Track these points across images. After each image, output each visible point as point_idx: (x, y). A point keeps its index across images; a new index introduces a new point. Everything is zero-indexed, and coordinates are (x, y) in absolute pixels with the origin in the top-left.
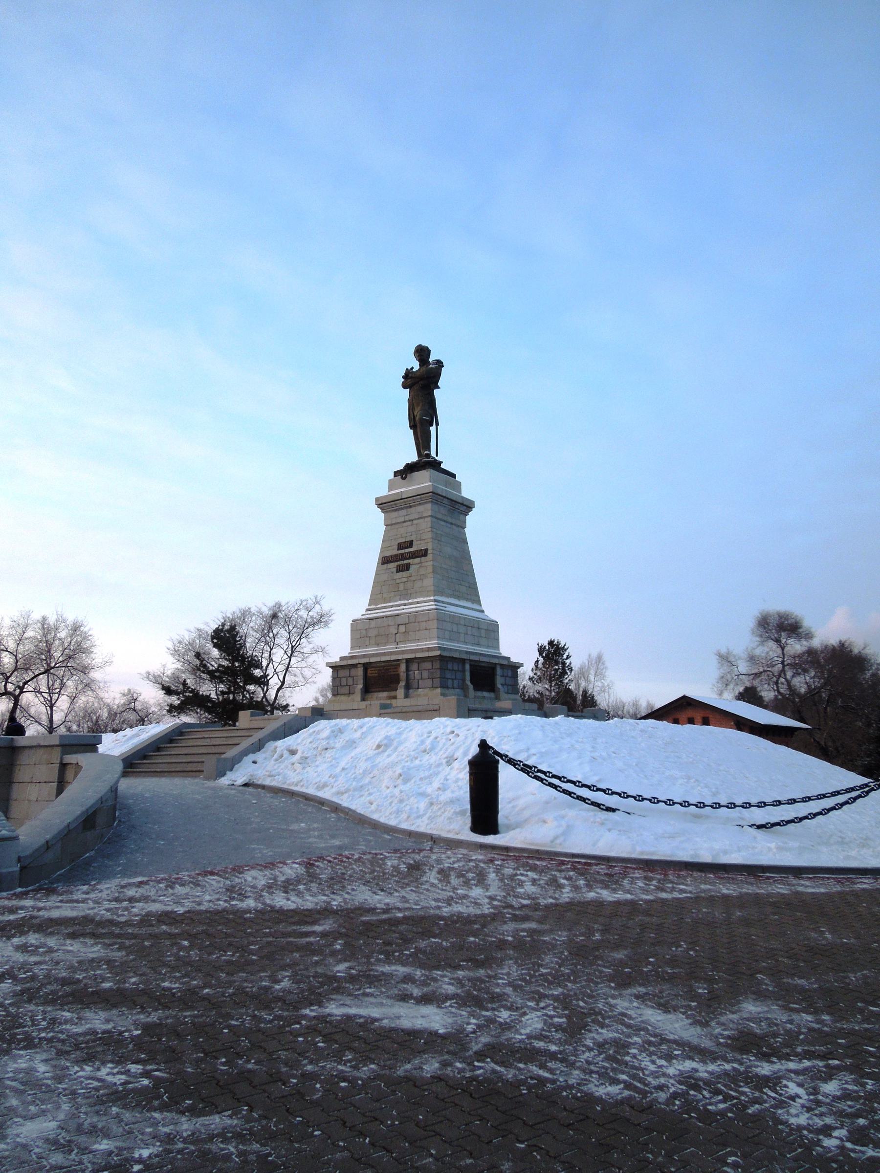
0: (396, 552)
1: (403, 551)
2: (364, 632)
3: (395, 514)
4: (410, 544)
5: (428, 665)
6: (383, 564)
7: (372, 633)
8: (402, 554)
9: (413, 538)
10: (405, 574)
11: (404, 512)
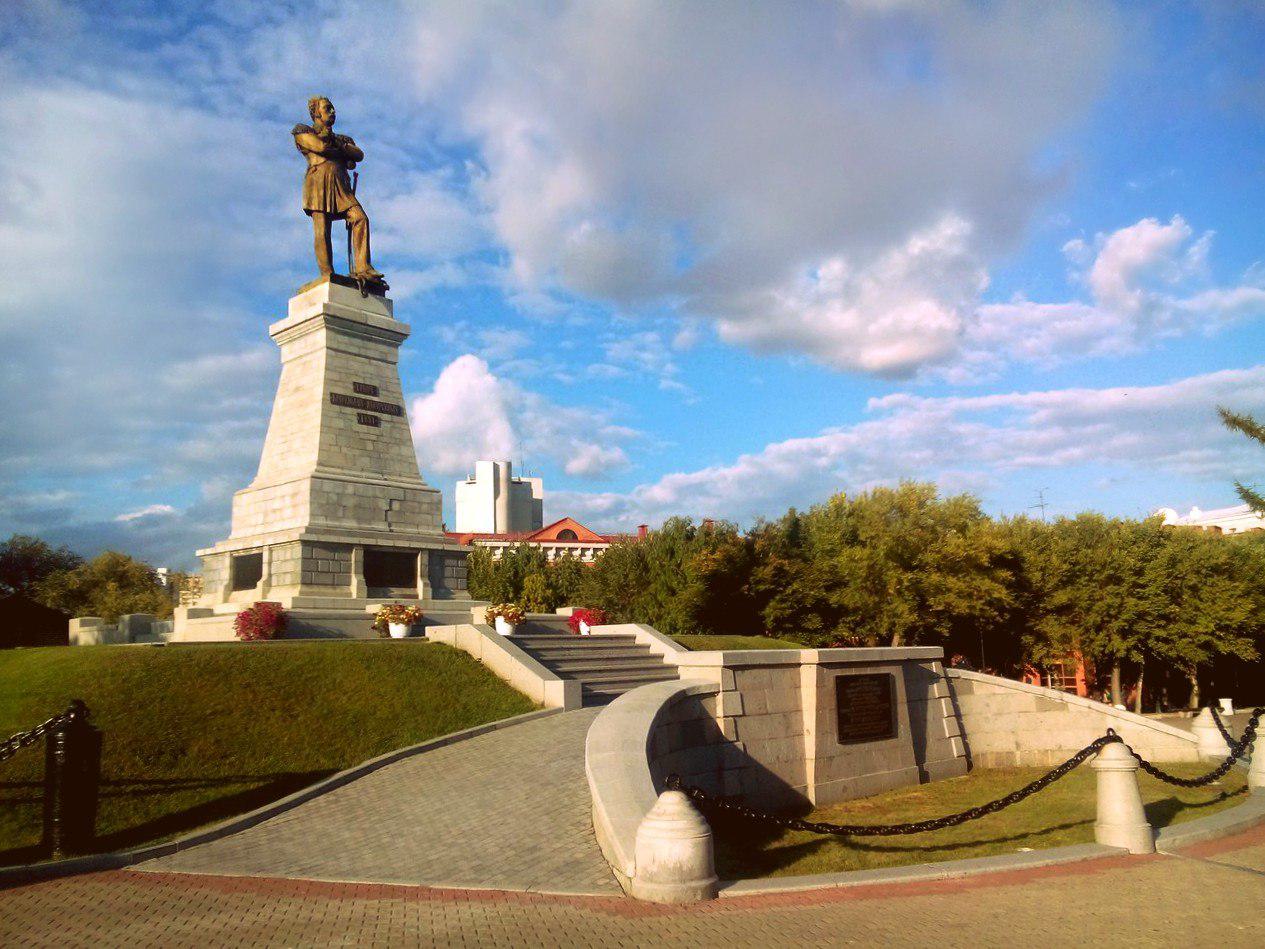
0: (349, 392)
1: (363, 396)
2: (335, 498)
3: (341, 338)
4: (374, 391)
7: (350, 502)
8: (365, 401)
9: (375, 383)
10: (372, 429)
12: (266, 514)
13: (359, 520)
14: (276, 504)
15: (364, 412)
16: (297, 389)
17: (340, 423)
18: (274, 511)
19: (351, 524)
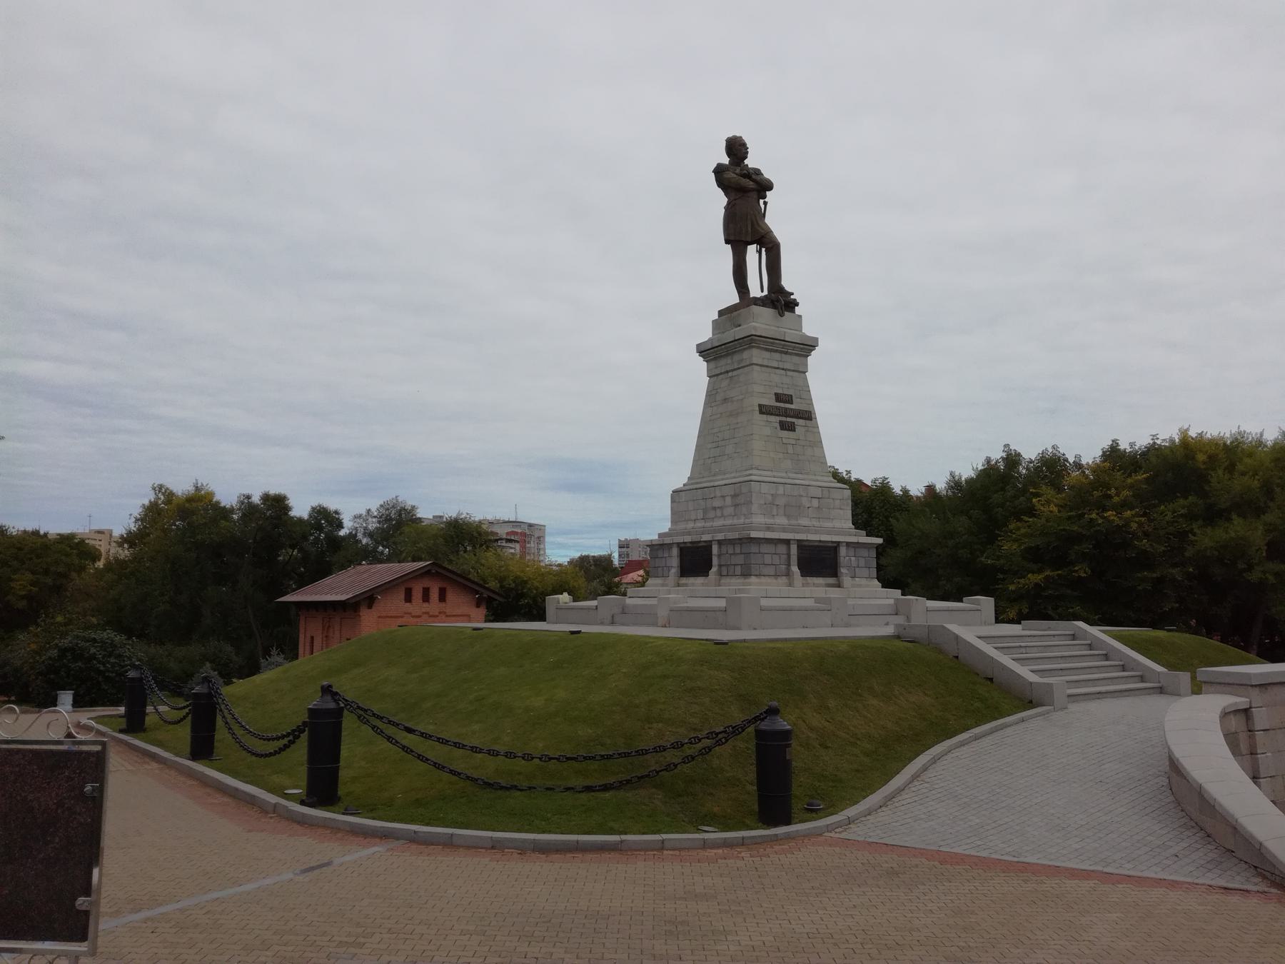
4: (789, 399)
5: (864, 553)
6: (761, 412)
7: (781, 501)
10: (791, 434)
11: (777, 356)
12: (705, 511)
13: (788, 517)
14: (717, 503)
15: (784, 419)
16: (725, 400)
17: (767, 431)
18: (715, 508)
19: (782, 520)
